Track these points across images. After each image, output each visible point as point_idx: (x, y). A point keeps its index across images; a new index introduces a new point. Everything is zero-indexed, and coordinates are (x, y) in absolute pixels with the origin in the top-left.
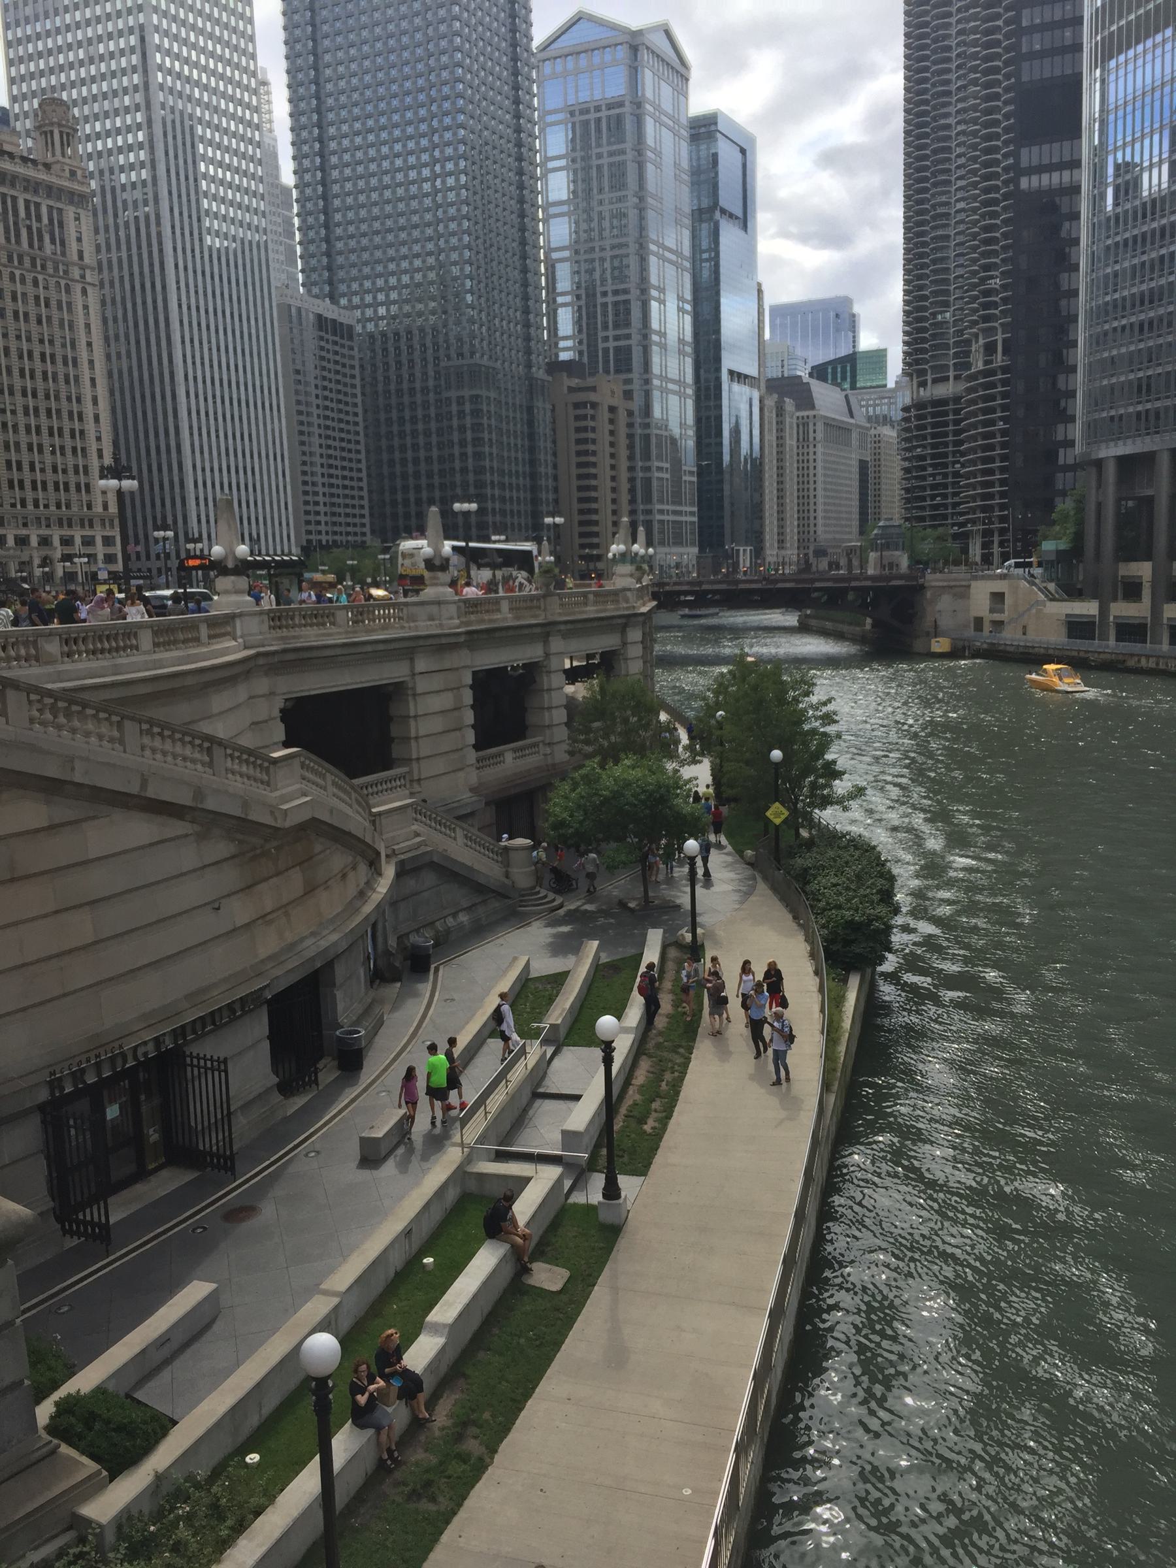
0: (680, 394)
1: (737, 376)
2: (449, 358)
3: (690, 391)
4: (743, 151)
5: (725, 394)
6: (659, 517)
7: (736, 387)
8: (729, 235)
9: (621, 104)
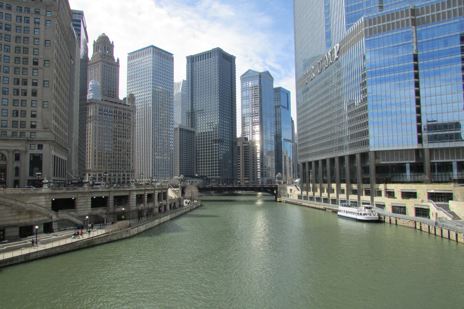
0: (270, 144)
1: (286, 140)
2: (214, 137)
3: (273, 143)
4: (287, 94)
5: (283, 144)
6: (264, 171)
7: (286, 142)
8: (283, 110)
9: (257, 86)
